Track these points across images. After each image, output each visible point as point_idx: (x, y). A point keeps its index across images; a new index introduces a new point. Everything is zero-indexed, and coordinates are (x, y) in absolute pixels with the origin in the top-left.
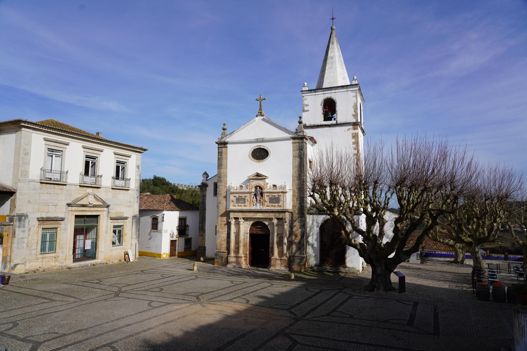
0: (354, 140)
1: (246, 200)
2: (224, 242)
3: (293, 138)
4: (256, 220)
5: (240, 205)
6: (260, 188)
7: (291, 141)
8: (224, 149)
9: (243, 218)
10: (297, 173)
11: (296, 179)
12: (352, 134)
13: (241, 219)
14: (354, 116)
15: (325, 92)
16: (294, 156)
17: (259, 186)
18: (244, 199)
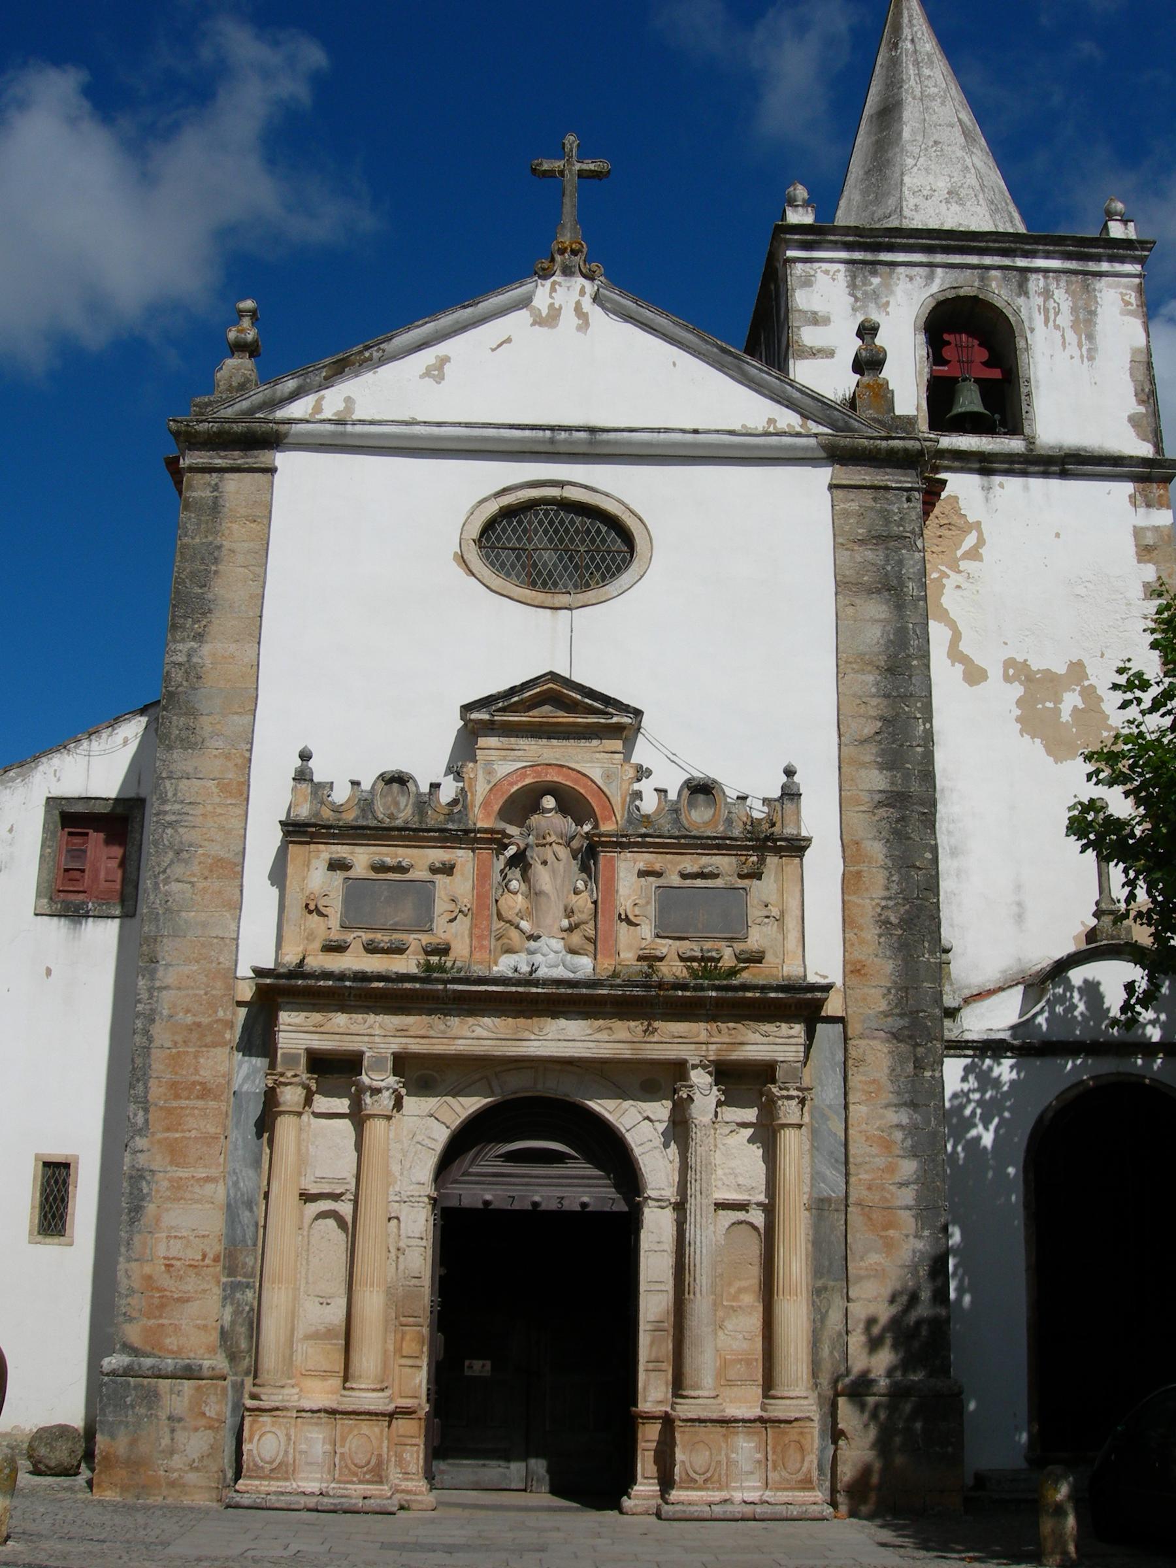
0: (1149, 573)
1: (441, 906)
2: (191, 1284)
3: (835, 455)
4: (518, 1085)
5: (382, 938)
6: (573, 804)
7: (824, 475)
8: (233, 484)
9: (402, 1063)
10: (876, 706)
11: (869, 754)
12: (1138, 532)
13: (378, 1065)
14: (1133, 420)
15: (939, 258)
16: (846, 586)
17: (553, 790)
18: (424, 895)
